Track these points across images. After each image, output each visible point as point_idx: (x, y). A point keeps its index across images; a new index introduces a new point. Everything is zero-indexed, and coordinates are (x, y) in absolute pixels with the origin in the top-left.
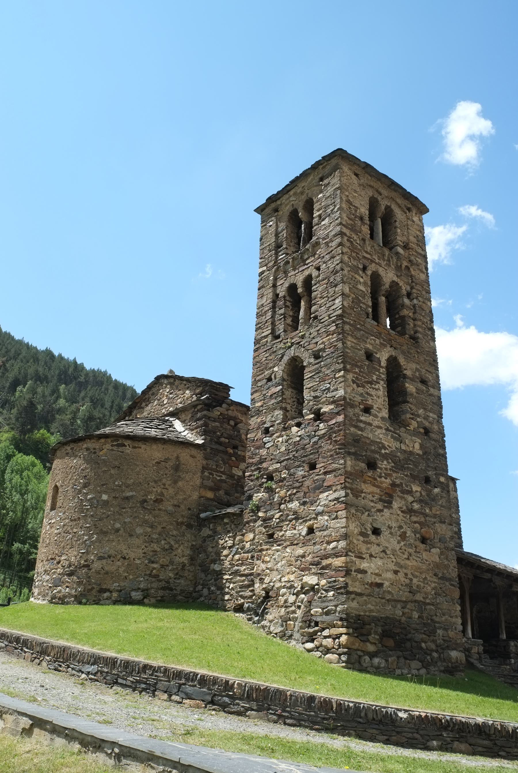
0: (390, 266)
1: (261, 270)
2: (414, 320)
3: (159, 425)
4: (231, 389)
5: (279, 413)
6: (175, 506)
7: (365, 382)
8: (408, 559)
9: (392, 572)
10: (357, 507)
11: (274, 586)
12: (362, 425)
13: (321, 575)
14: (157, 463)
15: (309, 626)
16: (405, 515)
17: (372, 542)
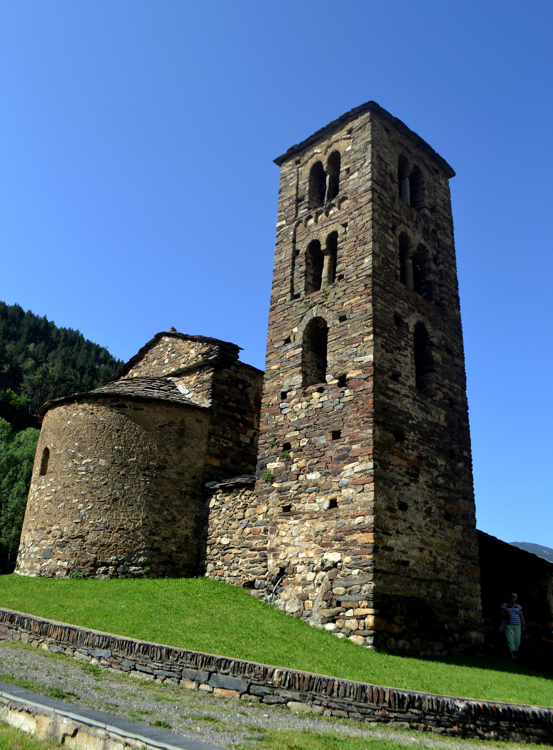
0: (417, 228)
2: (441, 286)
3: (161, 386)
4: (240, 351)
5: (298, 379)
6: (179, 473)
7: (393, 348)
8: (433, 536)
9: (418, 550)
10: (385, 480)
11: (289, 563)
12: (391, 393)
13: (344, 551)
14: (161, 426)
15: (330, 606)
16: (430, 490)
17: (399, 518)
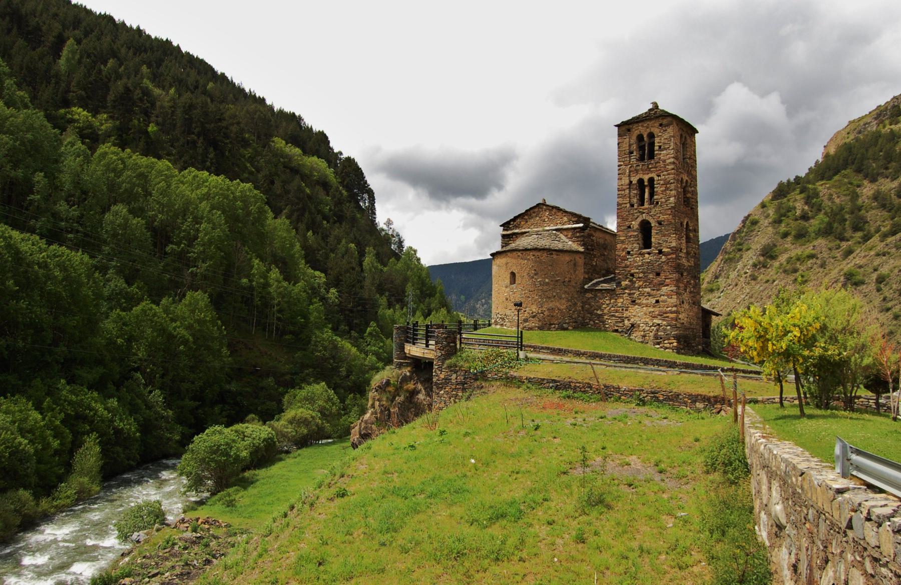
1: (620, 163)
